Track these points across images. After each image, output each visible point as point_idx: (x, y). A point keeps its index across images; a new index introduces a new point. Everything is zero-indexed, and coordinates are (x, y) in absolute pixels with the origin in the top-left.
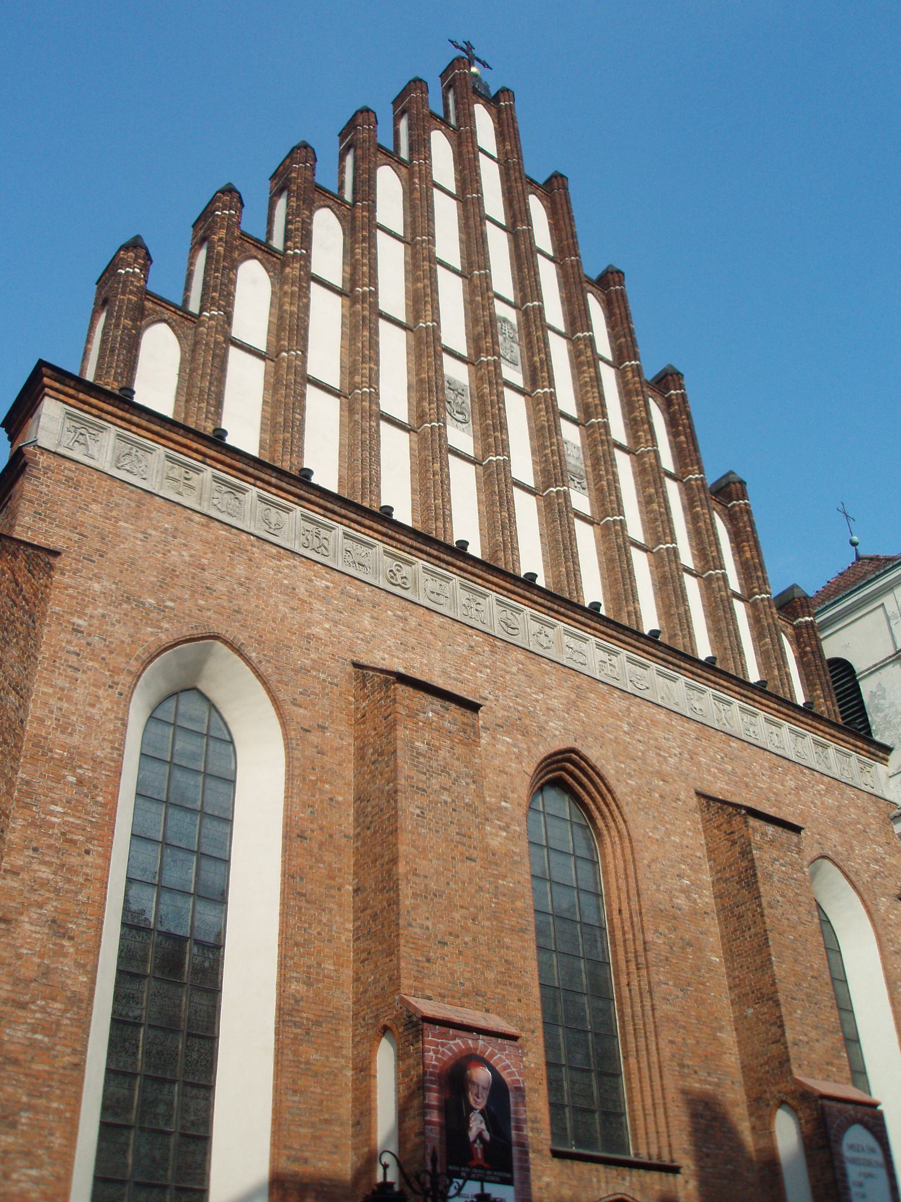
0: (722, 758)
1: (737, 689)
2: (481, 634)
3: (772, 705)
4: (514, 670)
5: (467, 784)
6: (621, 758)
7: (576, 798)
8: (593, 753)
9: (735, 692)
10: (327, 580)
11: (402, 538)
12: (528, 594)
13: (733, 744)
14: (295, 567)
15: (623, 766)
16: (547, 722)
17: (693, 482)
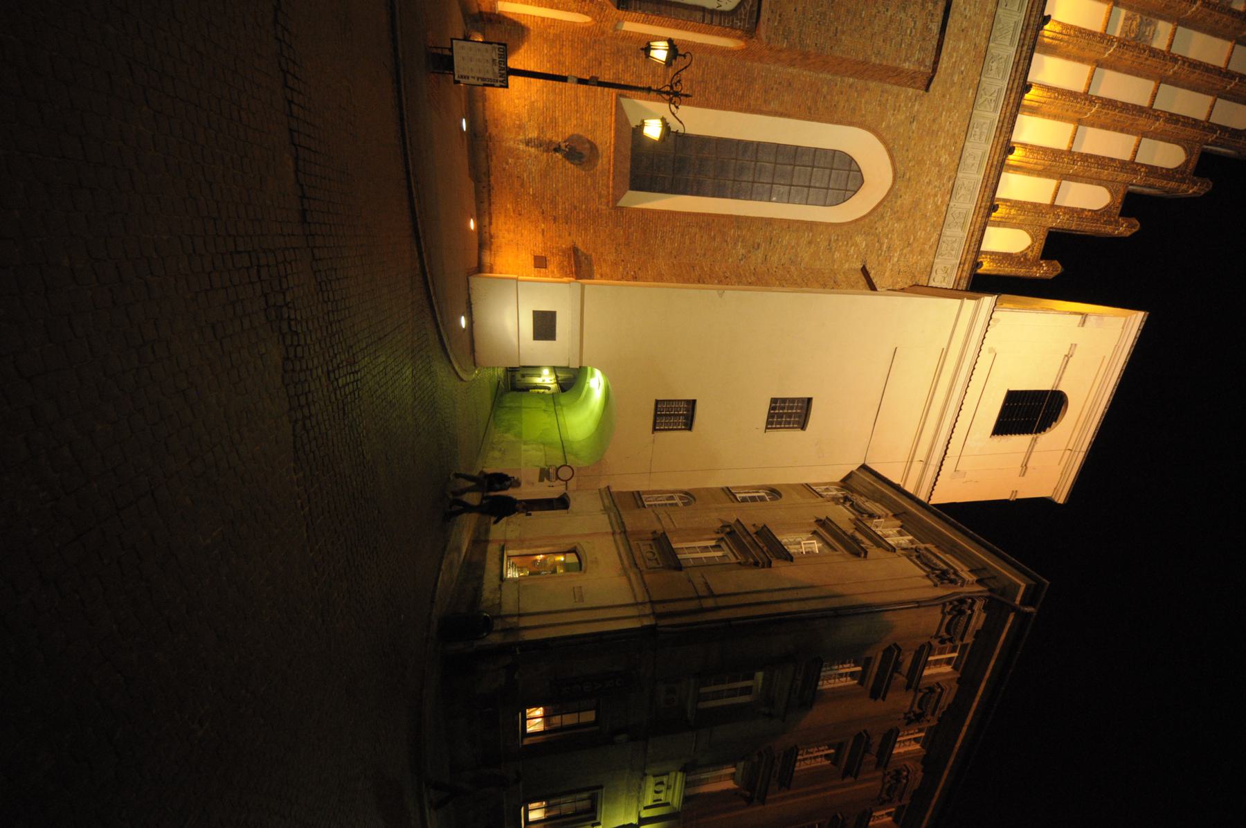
1: (1008, 114)
3: (996, 157)
13: (971, 91)
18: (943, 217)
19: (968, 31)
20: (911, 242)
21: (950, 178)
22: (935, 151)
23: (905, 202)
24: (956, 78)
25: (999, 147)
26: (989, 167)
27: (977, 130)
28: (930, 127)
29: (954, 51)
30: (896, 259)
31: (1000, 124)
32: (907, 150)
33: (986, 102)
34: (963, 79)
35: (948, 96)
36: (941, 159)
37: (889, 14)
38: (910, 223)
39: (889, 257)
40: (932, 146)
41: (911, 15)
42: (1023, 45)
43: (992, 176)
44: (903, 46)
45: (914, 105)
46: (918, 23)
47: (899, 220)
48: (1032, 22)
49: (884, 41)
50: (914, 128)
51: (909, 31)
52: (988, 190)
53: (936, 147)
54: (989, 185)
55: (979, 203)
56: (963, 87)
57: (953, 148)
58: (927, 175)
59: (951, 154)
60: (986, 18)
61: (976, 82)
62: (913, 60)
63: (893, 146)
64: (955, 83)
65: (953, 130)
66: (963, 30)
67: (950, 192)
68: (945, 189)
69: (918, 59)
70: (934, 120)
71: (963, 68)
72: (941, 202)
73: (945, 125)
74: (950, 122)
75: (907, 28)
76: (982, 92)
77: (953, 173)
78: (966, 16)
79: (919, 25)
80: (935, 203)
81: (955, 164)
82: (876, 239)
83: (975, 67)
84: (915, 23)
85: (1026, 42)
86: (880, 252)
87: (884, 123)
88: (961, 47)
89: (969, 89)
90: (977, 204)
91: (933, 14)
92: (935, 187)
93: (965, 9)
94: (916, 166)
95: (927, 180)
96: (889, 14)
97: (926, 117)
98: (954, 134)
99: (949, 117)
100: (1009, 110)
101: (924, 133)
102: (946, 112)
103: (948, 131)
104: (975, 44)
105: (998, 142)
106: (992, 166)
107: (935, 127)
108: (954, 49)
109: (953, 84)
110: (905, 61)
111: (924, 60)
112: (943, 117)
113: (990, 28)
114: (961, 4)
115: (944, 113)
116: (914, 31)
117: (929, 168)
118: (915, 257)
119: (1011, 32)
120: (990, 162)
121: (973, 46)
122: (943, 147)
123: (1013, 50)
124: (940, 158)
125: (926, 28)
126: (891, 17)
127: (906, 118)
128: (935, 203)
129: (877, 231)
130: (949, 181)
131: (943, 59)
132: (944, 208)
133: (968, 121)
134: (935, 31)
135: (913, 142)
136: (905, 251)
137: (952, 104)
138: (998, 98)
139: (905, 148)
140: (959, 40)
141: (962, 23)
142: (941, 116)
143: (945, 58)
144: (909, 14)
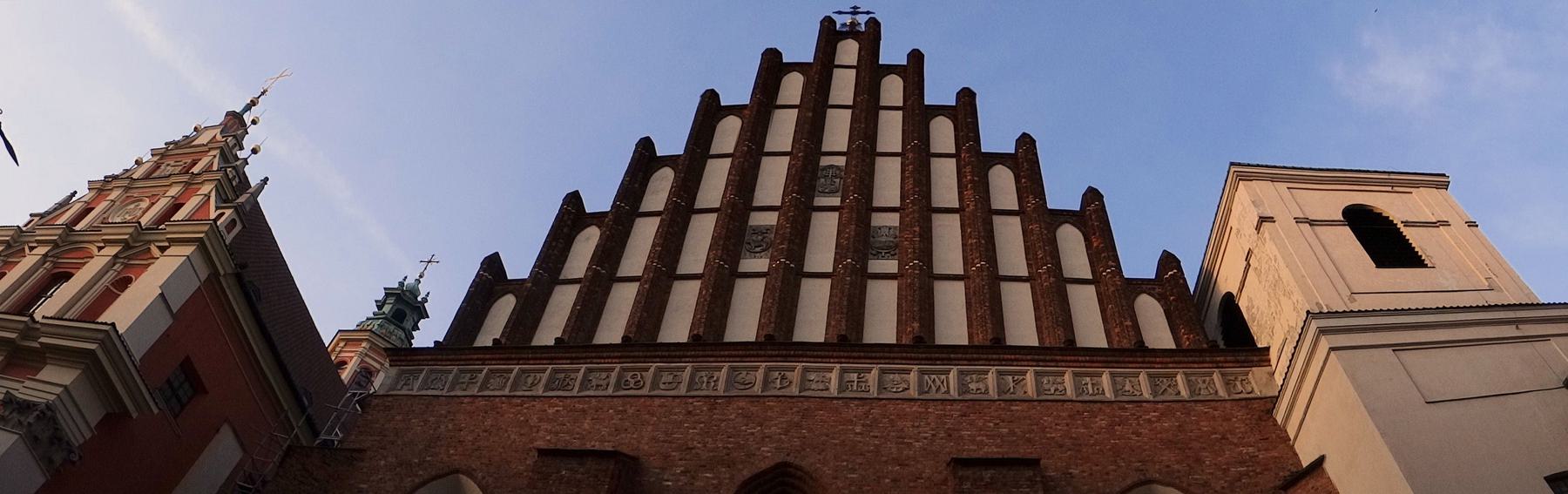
0: (996, 424)
1: (1029, 357)
6: (845, 457)
8: (808, 461)
9: (1028, 360)
11: (637, 354)
13: (1013, 408)
14: (533, 406)
18: (1173, 405)
19: (949, 429)
20: (1220, 437)
22: (1095, 436)
23: (1173, 459)
24: (1005, 431)
28: (1070, 450)
29: (974, 440)
30: (1251, 449)
38: (1195, 445)
39: (1253, 459)
42: (950, 359)
45: (1050, 476)
47: (1198, 460)
50: (1077, 472)
53: (1091, 436)
58: (1129, 438)
60: (929, 410)
64: (1010, 431)
66: (950, 436)
67: (1139, 404)
72: (1155, 412)
77: (1115, 406)
78: (933, 435)
80: (1159, 419)
81: (1103, 407)
82: (1238, 484)
83: (986, 410)
86: (1251, 474)
92: (1139, 424)
95: (1134, 437)
97: (1060, 458)
98: (1070, 416)
99: (1051, 428)
103: (1067, 425)
108: (973, 441)
109: (1012, 433)
112: (1053, 435)
113: (939, 402)
115: (1048, 435)
117: (1119, 439)
118: (1237, 425)
128: (1159, 419)
129: (1226, 485)
130: (1127, 408)
132: (1160, 406)
133: (1049, 403)
135: (1094, 468)
136: (1236, 441)
137: (1035, 427)
139: (1105, 477)
140: (961, 437)
142: (1054, 438)
143: (985, 450)
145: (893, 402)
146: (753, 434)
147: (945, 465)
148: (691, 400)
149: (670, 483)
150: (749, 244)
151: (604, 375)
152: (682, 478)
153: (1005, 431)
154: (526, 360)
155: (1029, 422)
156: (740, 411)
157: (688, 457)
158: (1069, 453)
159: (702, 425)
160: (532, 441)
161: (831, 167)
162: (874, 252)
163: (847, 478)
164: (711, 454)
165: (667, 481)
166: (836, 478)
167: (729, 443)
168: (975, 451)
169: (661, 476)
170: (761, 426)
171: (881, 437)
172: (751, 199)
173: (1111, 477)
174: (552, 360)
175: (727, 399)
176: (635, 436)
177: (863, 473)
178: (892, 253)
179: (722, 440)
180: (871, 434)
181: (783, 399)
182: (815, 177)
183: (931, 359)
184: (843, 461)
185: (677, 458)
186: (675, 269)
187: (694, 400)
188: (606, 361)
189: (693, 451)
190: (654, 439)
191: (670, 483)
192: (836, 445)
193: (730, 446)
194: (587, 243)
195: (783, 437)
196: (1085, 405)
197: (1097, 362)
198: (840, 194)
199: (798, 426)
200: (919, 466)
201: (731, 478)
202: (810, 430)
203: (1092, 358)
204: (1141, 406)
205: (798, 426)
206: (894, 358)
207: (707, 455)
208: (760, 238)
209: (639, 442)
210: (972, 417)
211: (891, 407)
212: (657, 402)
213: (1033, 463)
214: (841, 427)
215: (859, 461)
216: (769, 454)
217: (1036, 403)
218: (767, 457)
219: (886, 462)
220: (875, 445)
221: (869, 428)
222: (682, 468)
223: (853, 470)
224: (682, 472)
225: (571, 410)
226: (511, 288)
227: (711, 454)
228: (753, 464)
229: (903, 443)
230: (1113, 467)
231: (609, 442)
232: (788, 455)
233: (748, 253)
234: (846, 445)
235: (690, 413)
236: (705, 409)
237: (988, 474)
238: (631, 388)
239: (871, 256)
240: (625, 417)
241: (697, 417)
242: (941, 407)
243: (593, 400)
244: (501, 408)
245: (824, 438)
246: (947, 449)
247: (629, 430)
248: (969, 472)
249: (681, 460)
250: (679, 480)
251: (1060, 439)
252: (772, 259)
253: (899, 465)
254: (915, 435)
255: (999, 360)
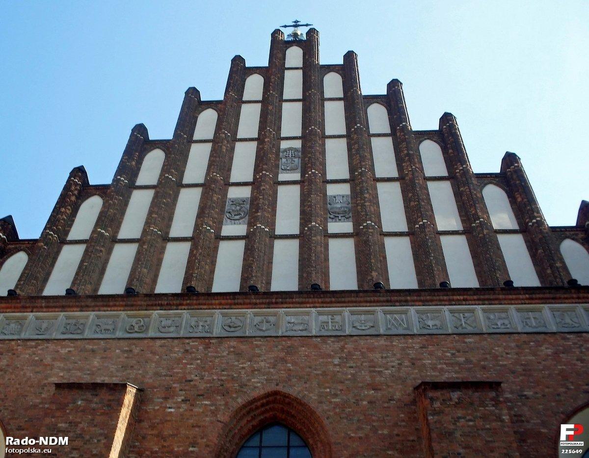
0: (453, 354)
1: (475, 297)
2: (198, 340)
3: (521, 297)
4: (225, 354)
5: (99, 441)
6: (327, 385)
7: (291, 430)
8: (295, 390)
9: (474, 300)
10: (71, 347)
12: (247, 301)
13: (467, 340)
15: (328, 390)
16: (249, 380)
17: (458, 174)
21: (564, 339)
22: (544, 363)
24: (462, 359)
25: (511, 297)
26: (534, 302)
27: (499, 324)
29: (436, 368)
31: (486, 302)
32: (559, 395)
33: (468, 322)
34: (459, 352)
35: (482, 363)
36: (550, 353)
37: (461, 451)
40: (541, 367)
41: (453, 424)
42: (406, 301)
43: (541, 296)
44: (488, 426)
46: (459, 415)
48: (385, 299)
49: (492, 451)
50: (531, 393)
51: (471, 423)
52: (558, 296)
53: (539, 363)
54: (552, 296)
55: (574, 301)
56: (467, 350)
57: (531, 344)
58: (575, 365)
59: (539, 344)
61: (457, 338)
62: (497, 411)
63: (562, 413)
64: (466, 359)
65: (513, 349)
67: (579, 334)
68: (579, 341)
69: (493, 406)
70: (513, 372)
71: (449, 354)
73: (511, 358)
74: (507, 354)
75: (469, 426)
76: (460, 328)
77: (557, 336)
78: (399, 364)
79: (460, 413)
81: (547, 337)
84: (459, 418)
85: (403, 298)
87: (543, 430)
88: (430, 362)
89: (465, 342)
90: (576, 303)
91: (443, 400)
93: (393, 367)
94: (571, 380)
95: (579, 363)
96: (461, 451)
99: (502, 356)
100: (471, 297)
101: (532, 380)
102: (500, 361)
104: (421, 348)
105: (505, 299)
106: (532, 299)
107: (519, 369)
108: (434, 369)
109: (468, 361)
110: (502, 421)
111: (492, 399)
112: (505, 363)
113: (402, 337)
114: (390, 372)
116: (468, 418)
119: (395, 316)
120: (527, 302)
121: (424, 349)
122: (535, 355)
123: (412, 310)
124: (548, 355)
125: (458, 404)
126: (463, 448)
127: (524, 405)
130: (568, 339)
131: (448, 378)
133: (499, 336)
134: (459, 393)
135: (547, 390)
137: (488, 356)
138: (459, 311)
139: (557, 398)
140: (424, 365)
141: (407, 367)
142: (506, 365)
144: (452, 427)
145: (362, 338)
146: (243, 368)
147: (411, 389)
148: (187, 341)
149: (172, 410)
150: (229, 212)
151: (110, 321)
152: (183, 405)
153: (462, 359)
154: (40, 309)
155: (482, 351)
156: (232, 349)
157: (187, 388)
158: (521, 378)
159: (199, 361)
160: (46, 378)
161: (290, 149)
162: (332, 216)
163: (331, 402)
164: (208, 385)
165: (170, 408)
166: (321, 402)
167: (223, 375)
168: (437, 376)
169: (164, 405)
170: (250, 361)
171: (356, 367)
172: (229, 176)
173: (562, 398)
174: (63, 308)
175: (220, 339)
176: (140, 372)
177: (345, 397)
178: (347, 216)
179: (217, 374)
180: (348, 365)
181: (269, 339)
182: (278, 158)
183: (391, 301)
184: (325, 388)
185: (178, 389)
186: (168, 233)
187: (191, 341)
188: (113, 308)
189: (192, 383)
190: (157, 374)
191: (172, 410)
192: (317, 375)
193: (223, 378)
194: (91, 208)
195: (272, 370)
196: (530, 336)
197: (536, 299)
198: (299, 170)
199: (283, 360)
200: (390, 390)
201: (226, 404)
202: (295, 363)
203: (531, 296)
204: (581, 337)
205: (283, 360)
206: (360, 302)
207: (205, 385)
208: (238, 208)
209: (144, 377)
210: (431, 348)
211: (362, 342)
212: (158, 343)
213: (494, 386)
214: (321, 360)
215: (340, 388)
216: (259, 385)
217: (486, 336)
218: (257, 387)
219: (362, 387)
220: (353, 375)
221: (345, 360)
222: (183, 398)
223: (336, 395)
224: (183, 400)
225: (81, 351)
226: (23, 246)
227: (208, 385)
228: (246, 392)
229: (374, 371)
230: (563, 390)
231: (117, 376)
232: (277, 385)
233: (229, 220)
234: (327, 375)
235: (187, 351)
236: (201, 348)
237: (455, 395)
238: (136, 332)
239: (330, 220)
240: (131, 355)
241: (193, 355)
242: (403, 341)
243: (102, 342)
244: (17, 350)
245: (308, 370)
246: (413, 376)
247: (136, 367)
248: (438, 394)
249: (181, 390)
250: (179, 408)
251: (511, 366)
252: (250, 224)
253: (373, 390)
254: (384, 364)
255: (450, 300)
